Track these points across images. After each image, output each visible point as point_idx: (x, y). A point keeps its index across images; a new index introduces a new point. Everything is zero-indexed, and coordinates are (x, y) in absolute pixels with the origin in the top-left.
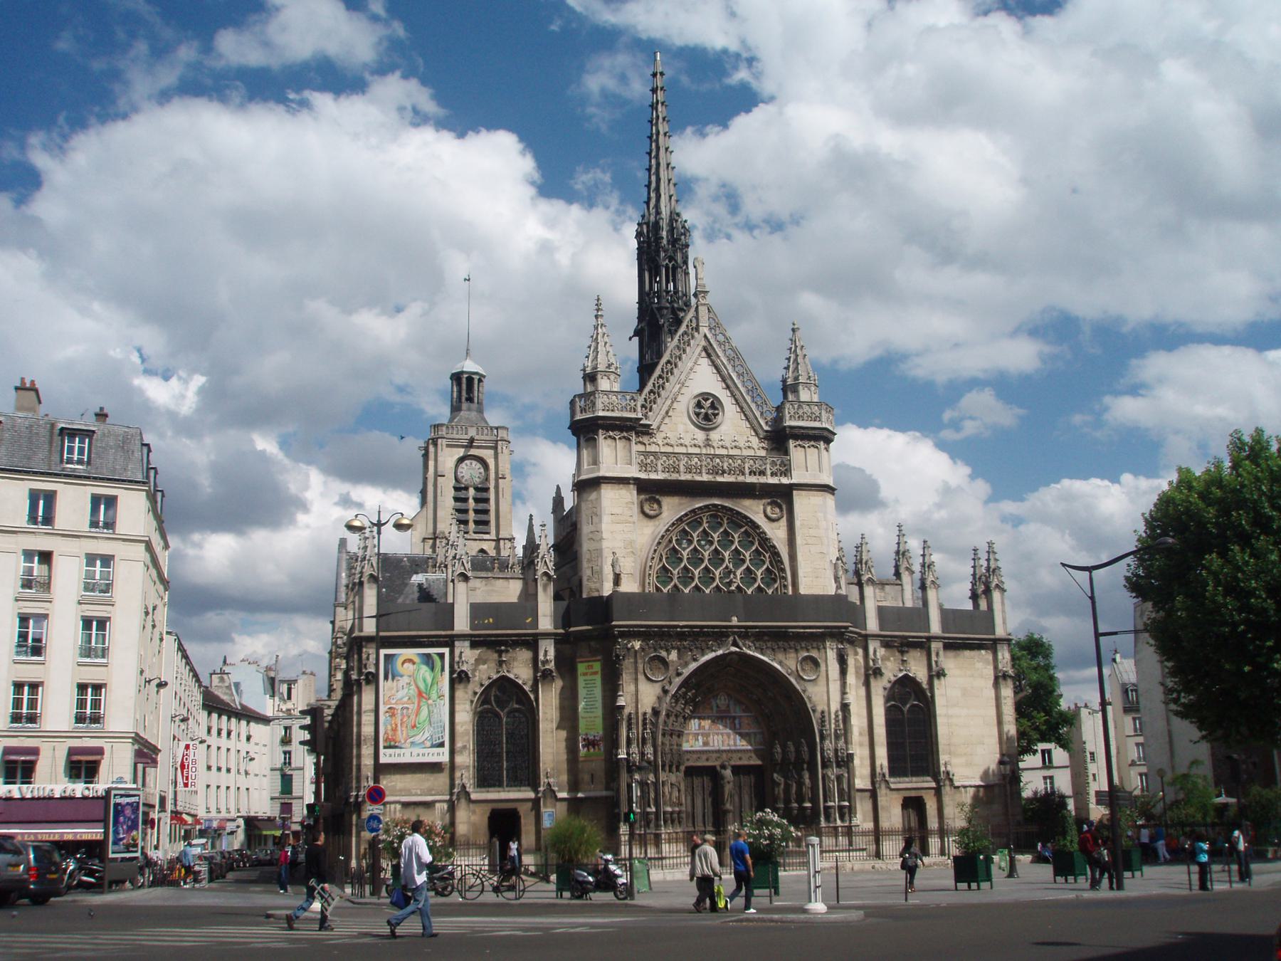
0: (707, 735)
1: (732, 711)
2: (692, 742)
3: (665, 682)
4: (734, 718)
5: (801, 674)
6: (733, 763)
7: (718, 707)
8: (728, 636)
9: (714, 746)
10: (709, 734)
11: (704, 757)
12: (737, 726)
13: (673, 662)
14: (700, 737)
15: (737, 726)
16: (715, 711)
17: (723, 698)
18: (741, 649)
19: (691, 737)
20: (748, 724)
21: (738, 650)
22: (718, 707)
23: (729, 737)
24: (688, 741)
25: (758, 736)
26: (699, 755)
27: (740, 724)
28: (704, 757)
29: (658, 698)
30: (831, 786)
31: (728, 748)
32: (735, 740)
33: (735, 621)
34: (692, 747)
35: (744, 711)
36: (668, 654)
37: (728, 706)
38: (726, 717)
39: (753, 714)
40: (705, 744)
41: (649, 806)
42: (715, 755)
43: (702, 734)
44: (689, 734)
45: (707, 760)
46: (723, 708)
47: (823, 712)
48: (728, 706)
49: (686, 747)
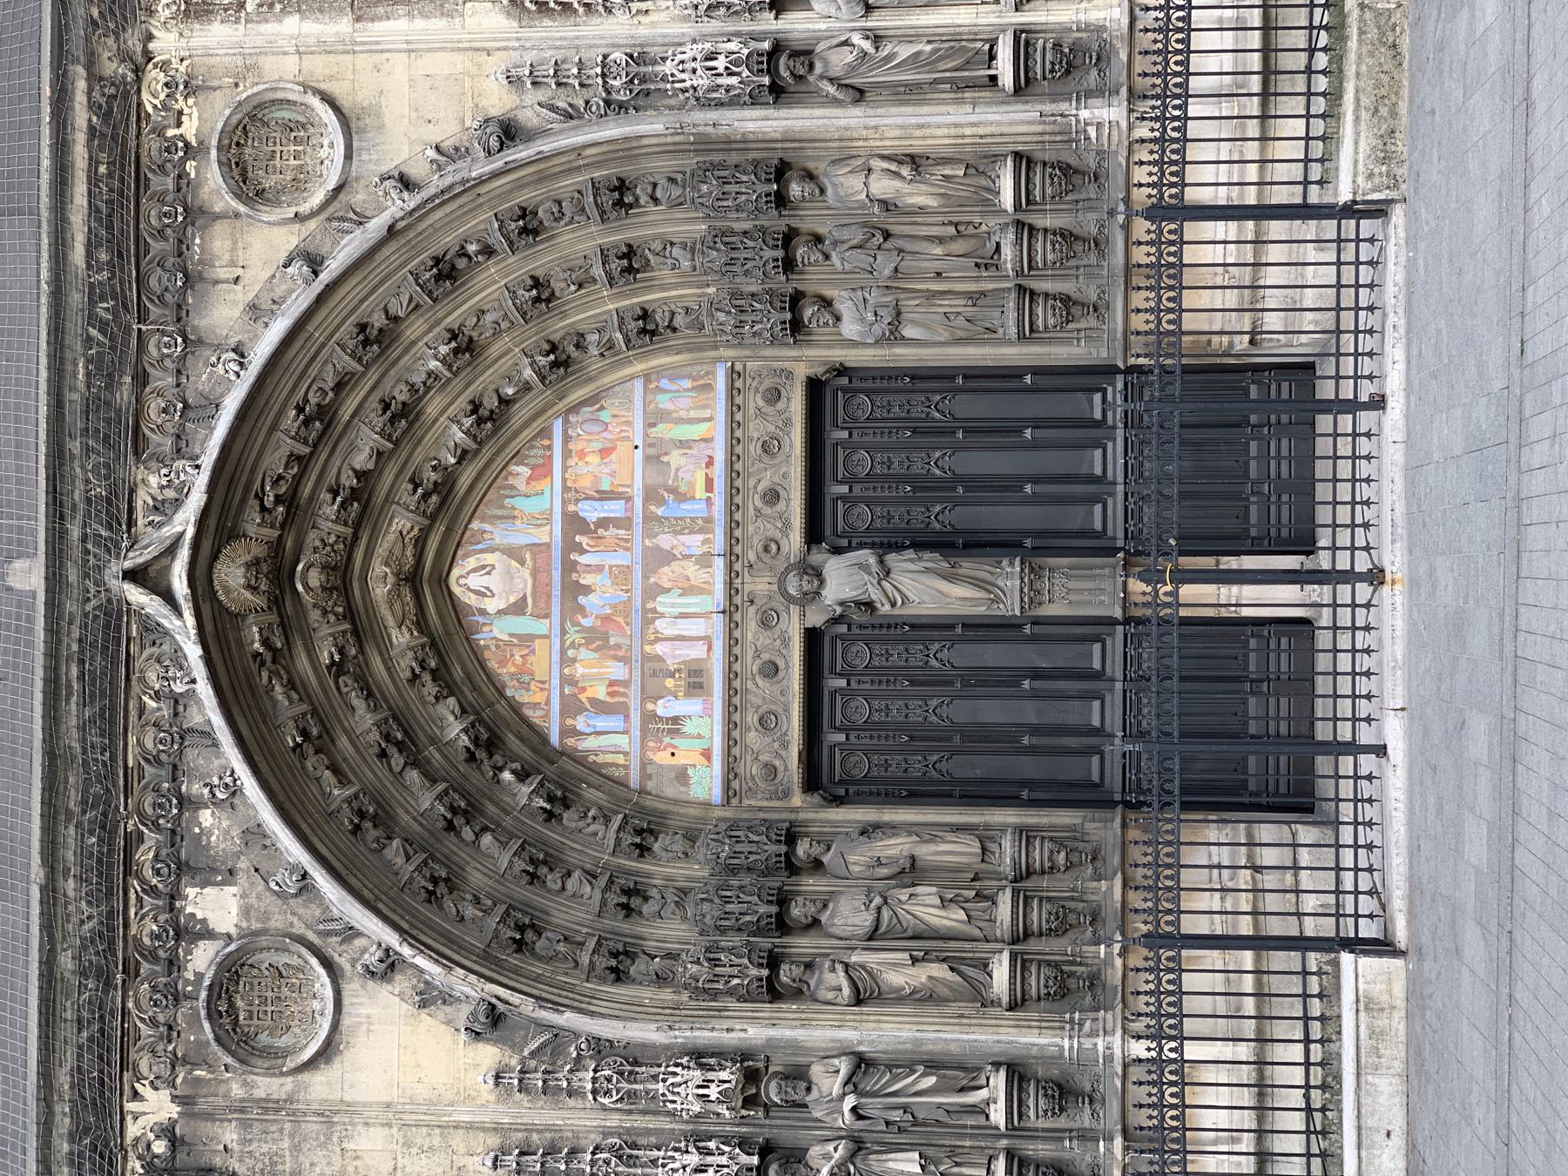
0: (654, 670)
1: (541, 536)
2: (686, 753)
3: (343, 961)
4: (574, 523)
5: (317, 198)
6: (795, 540)
7: (518, 608)
8: (114, 614)
9: (708, 640)
10: (646, 658)
11: (760, 691)
12: (614, 509)
13: (246, 912)
14: (663, 708)
15: (614, 509)
16: (540, 627)
17: (475, 581)
18: (171, 550)
19: (662, 758)
20: (605, 452)
21: (184, 554)
22: (518, 608)
23: (667, 557)
24: (682, 776)
25: (663, 401)
26: (752, 719)
27: (604, 496)
28: (760, 691)
29: (423, 1005)
30: (905, 52)
31: (719, 563)
32: (680, 526)
33: (29, 576)
34: (707, 754)
35: (542, 471)
36: (209, 934)
37: (513, 553)
38: (569, 567)
39: (558, 426)
40: (695, 682)
41: (981, 1110)
42: (751, 630)
43: (649, 696)
44: (645, 764)
45: (771, 670)
46: (523, 581)
47: (513, 80)
48: (513, 553)
49: (706, 784)
